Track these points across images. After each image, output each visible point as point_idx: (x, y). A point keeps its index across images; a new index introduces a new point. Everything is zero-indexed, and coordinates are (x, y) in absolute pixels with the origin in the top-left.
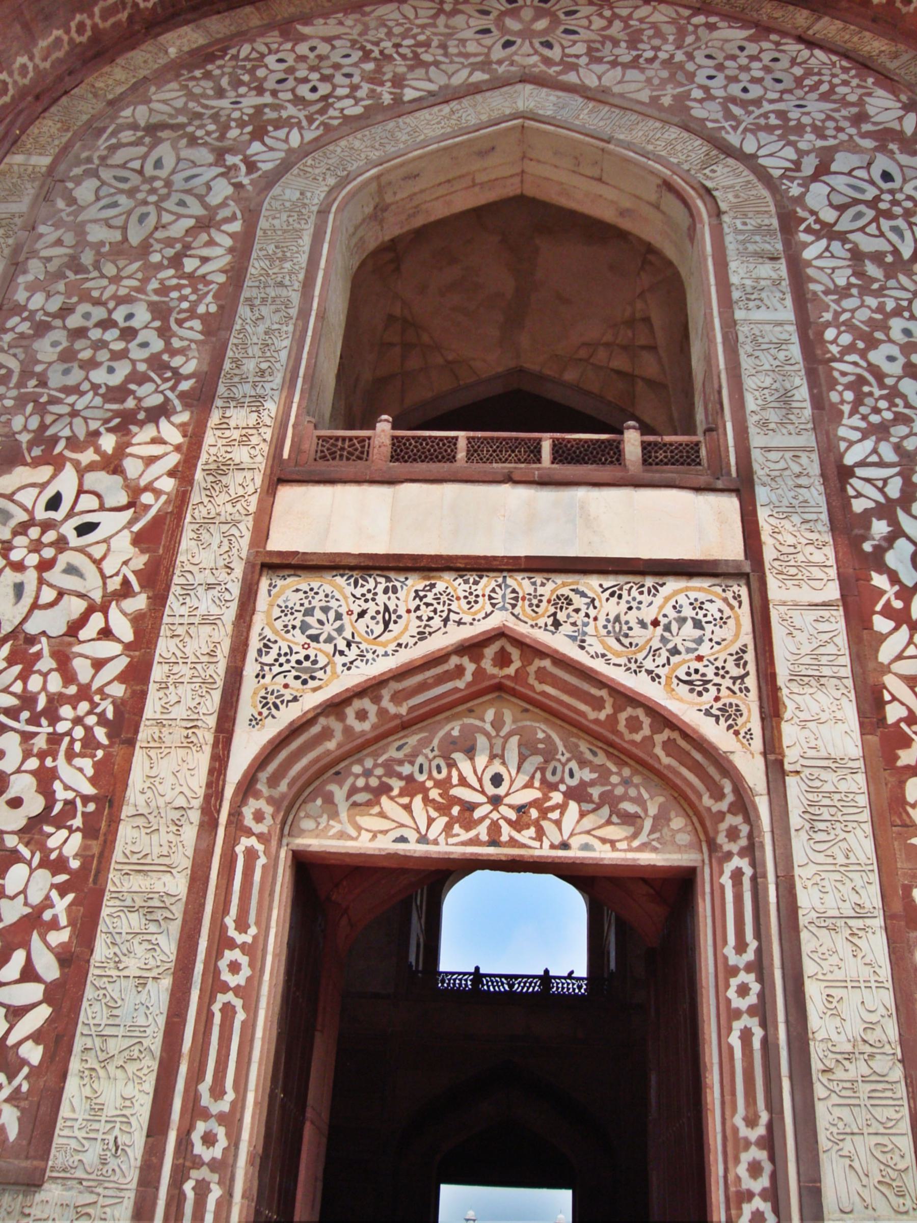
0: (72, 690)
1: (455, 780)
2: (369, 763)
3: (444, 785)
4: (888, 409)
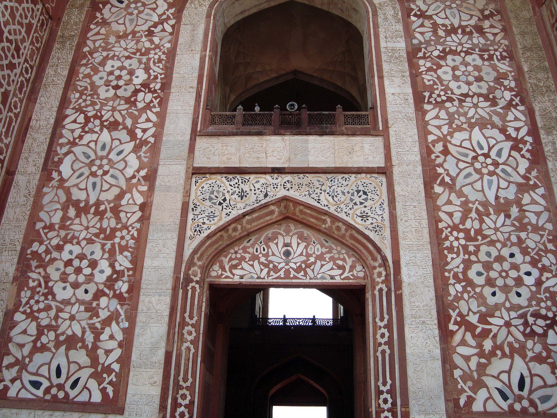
0: (119, 226)
1: (270, 254)
2: (236, 249)
3: (266, 256)
4: (444, 95)
